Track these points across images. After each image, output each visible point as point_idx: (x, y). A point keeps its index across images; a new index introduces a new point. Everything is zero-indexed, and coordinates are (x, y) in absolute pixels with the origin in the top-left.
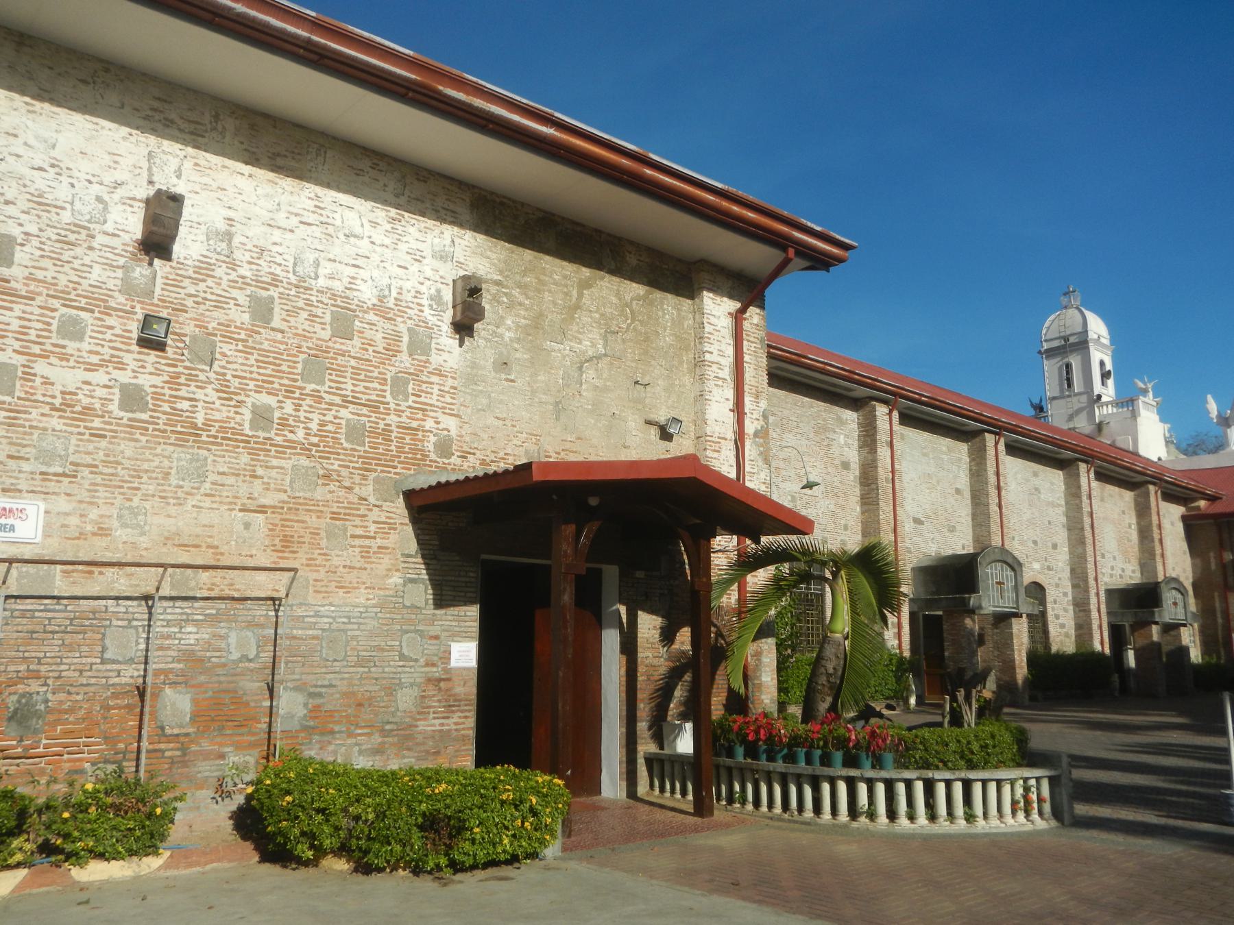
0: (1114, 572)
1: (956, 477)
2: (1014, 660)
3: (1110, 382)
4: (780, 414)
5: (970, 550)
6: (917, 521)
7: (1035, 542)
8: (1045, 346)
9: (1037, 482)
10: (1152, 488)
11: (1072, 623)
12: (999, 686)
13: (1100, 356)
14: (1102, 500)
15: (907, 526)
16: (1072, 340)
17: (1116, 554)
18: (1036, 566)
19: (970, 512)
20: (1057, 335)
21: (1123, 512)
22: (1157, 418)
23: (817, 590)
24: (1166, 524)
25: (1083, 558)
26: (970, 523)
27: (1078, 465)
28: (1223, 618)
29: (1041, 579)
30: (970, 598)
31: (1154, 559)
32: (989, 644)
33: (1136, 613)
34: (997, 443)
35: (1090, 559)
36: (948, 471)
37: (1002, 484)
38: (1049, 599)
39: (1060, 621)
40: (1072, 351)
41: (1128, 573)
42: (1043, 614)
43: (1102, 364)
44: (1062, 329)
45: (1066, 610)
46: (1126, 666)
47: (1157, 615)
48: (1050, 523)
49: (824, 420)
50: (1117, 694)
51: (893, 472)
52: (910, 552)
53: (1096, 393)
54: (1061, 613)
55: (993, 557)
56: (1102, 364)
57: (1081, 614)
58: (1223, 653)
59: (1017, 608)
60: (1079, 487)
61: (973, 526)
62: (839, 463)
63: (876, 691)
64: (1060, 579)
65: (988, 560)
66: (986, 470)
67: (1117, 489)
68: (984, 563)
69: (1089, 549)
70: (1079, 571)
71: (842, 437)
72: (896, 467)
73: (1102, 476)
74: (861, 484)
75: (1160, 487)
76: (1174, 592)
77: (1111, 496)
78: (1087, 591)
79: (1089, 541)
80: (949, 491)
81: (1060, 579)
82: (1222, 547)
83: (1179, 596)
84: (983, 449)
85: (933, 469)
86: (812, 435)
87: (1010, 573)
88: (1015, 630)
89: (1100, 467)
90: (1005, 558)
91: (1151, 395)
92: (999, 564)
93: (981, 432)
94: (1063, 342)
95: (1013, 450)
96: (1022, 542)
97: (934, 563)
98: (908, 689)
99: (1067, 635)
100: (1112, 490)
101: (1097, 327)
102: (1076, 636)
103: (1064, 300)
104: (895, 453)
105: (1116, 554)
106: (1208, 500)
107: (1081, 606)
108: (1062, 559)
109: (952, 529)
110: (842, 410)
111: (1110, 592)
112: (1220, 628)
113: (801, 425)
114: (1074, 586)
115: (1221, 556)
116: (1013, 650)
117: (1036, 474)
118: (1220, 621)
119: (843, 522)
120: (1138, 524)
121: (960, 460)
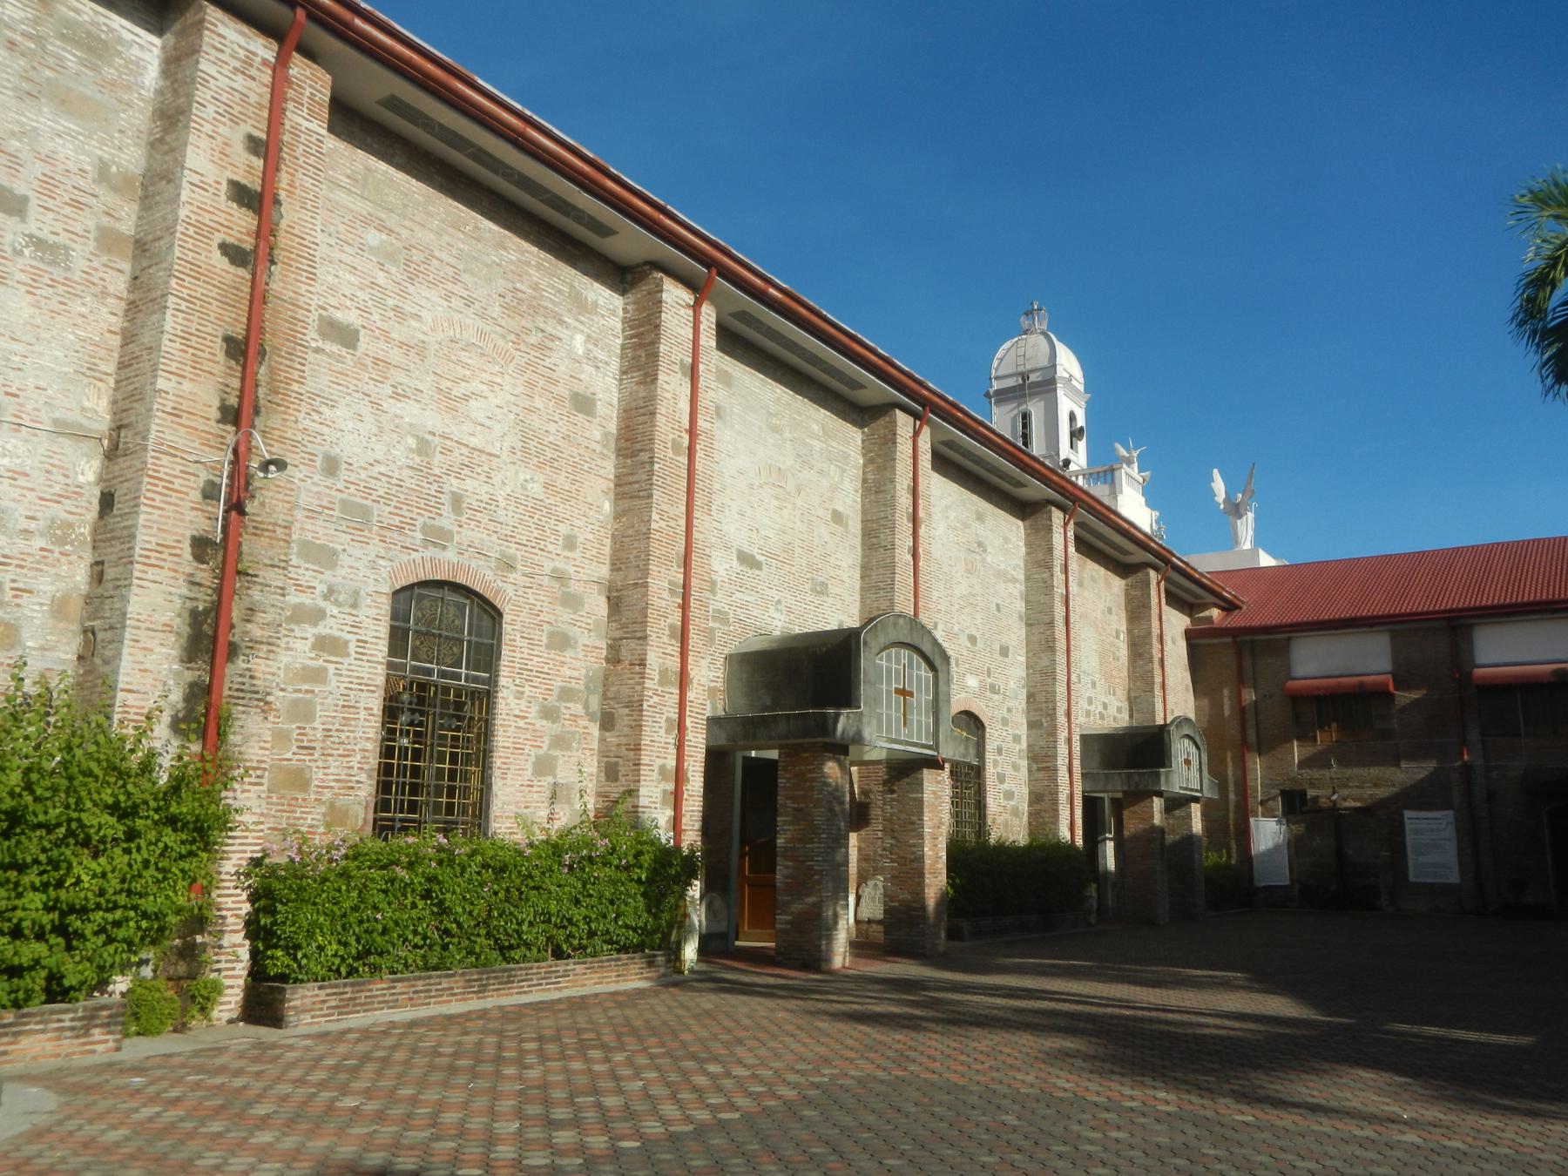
0: (1092, 708)
1: (834, 488)
2: (920, 859)
3: (1082, 445)
4: (405, 233)
5: (853, 622)
6: (746, 560)
7: (972, 639)
8: (996, 385)
9: (982, 531)
10: (1152, 574)
12: (886, 912)
13: (1070, 404)
14: (1081, 584)
15: (721, 565)
16: (1033, 378)
18: (972, 682)
19: (859, 561)
20: (1012, 370)
21: (1110, 611)
22: (1142, 500)
23: (476, 680)
25: (1050, 675)
26: (858, 584)
27: (1050, 511)
28: (1236, 794)
29: (978, 708)
30: (837, 716)
31: (1152, 691)
32: (877, 825)
34: (916, 434)
35: (1062, 677)
36: (821, 472)
37: (921, 514)
38: (990, 746)
39: (1006, 786)
41: (1112, 711)
42: (978, 772)
43: (1072, 417)
44: (1021, 360)
45: (1016, 767)
46: (1101, 868)
47: (1163, 779)
48: (998, 608)
49: (535, 287)
50: (1093, 921)
51: (692, 432)
52: (725, 621)
53: (1063, 457)
54: (1009, 771)
55: (893, 636)
56: (1072, 417)
57: (1041, 775)
58: (1234, 846)
59: (937, 749)
60: (1050, 550)
61: (862, 588)
62: (566, 394)
63: (591, 934)
64: (1009, 710)
65: (883, 639)
66: (892, 481)
67: (1102, 570)
68: (874, 646)
69: (1061, 659)
70: (1041, 697)
71: (579, 338)
72: (702, 423)
73: (1087, 547)
74: (620, 452)
76: (1186, 741)
77: (1094, 580)
78: (1053, 733)
79: (1061, 645)
80: (821, 512)
81: (1009, 710)
82: (1241, 681)
83: (1193, 750)
84: (890, 440)
85: (790, 462)
86: (496, 310)
87: (925, 673)
88: (928, 796)
90: (916, 641)
91: (1136, 466)
92: (904, 653)
93: (887, 408)
94: (1020, 381)
95: (945, 463)
96: (951, 635)
97: (774, 646)
98: (680, 923)
99: (1015, 812)
100: (1095, 570)
101: (1068, 364)
102: (1030, 814)
103: (1025, 322)
104: (701, 395)
105: (1097, 677)
106: (1223, 609)
107: (1041, 760)
108: (1014, 674)
109: (821, 590)
110: (586, 280)
111: (1084, 738)
112: (1232, 808)
113: (466, 278)
114: (1032, 725)
115: (1239, 696)
116: (921, 837)
117: (980, 517)
118: (1232, 796)
119: (564, 529)
120: (1129, 631)
121: (846, 457)
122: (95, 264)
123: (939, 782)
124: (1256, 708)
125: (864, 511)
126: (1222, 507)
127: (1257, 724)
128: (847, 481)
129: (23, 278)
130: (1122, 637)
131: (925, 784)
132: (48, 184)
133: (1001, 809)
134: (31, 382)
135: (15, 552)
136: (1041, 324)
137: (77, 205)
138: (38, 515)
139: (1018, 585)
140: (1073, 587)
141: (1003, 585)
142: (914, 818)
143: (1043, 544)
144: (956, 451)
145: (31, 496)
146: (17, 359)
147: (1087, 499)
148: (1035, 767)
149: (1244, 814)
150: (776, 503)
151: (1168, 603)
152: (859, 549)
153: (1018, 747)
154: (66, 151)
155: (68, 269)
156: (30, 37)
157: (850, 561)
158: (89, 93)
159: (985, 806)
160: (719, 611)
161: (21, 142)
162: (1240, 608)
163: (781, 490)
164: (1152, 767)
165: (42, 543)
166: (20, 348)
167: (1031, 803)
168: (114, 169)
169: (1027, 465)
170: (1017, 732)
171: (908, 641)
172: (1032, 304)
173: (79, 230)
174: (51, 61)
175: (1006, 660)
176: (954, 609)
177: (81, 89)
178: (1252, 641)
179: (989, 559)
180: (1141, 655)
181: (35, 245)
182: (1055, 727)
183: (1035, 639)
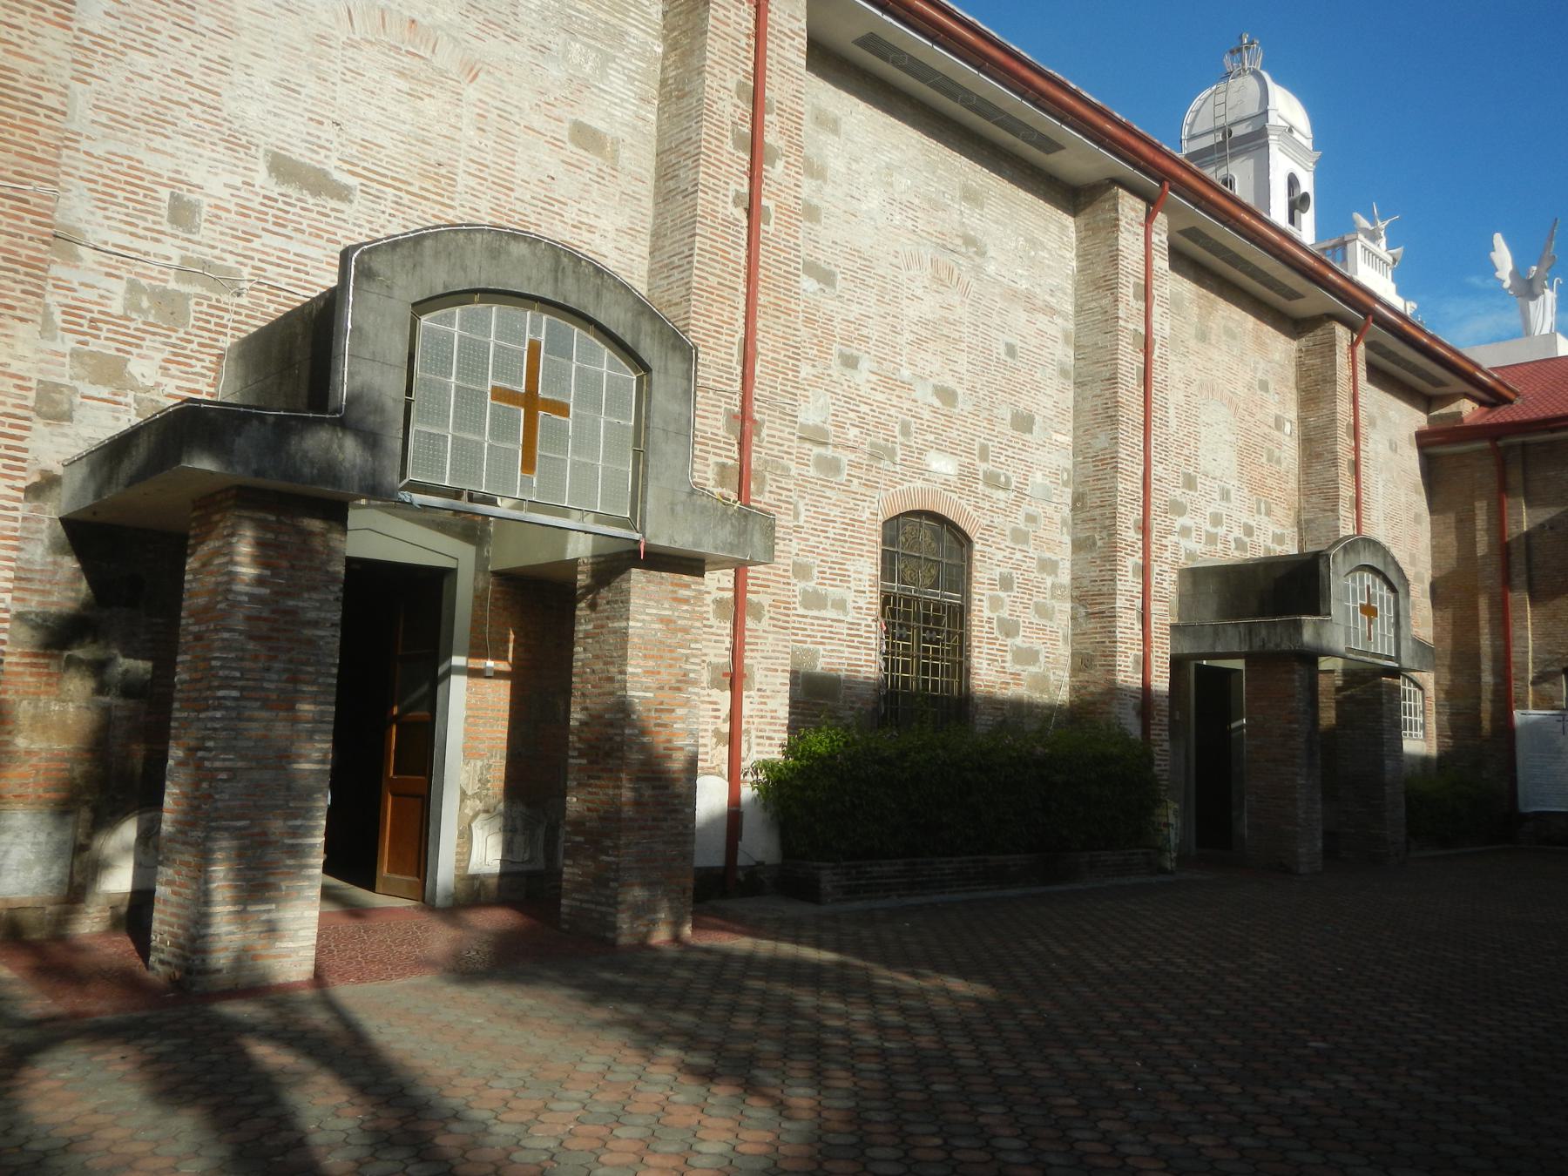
0: (1221, 531)
6: (283, 168)
9: (974, 221)
10: (1342, 333)
11: (1064, 651)
14: (1203, 336)
16: (1238, 131)
17: (1232, 484)
18: (943, 465)
20: (1209, 126)
24: (1375, 446)
27: (1116, 197)
28: (1495, 673)
31: (1335, 510)
33: (1250, 626)
35: (1131, 467)
36: (543, 49)
37: (771, 137)
38: (983, 575)
39: (1019, 641)
40: (1233, 156)
42: (959, 615)
43: (1293, 182)
44: (1220, 110)
45: (1042, 611)
48: (1011, 351)
56: (1293, 182)
57: (1092, 625)
59: (642, 531)
60: (1114, 259)
64: (1031, 518)
65: (439, 279)
69: (1131, 438)
70: (1093, 499)
75: (1370, 346)
76: (1368, 578)
78: (1110, 558)
79: (1132, 410)
80: (537, 121)
83: (1381, 591)
89: (1193, 234)
91: (1383, 242)
92: (535, 326)
101: (1287, 109)
105: (1232, 484)
106: (1482, 403)
114: (1079, 546)
117: (971, 196)
118: (1487, 678)
120: (1302, 420)
123: (686, 601)
124: (1528, 549)
125: (660, 139)
126: (1507, 284)
127: (1529, 570)
128: (616, 82)
130: (1288, 428)
131: (635, 602)
133: (1008, 678)
136: (1254, 59)
139: (1059, 321)
140: (1162, 325)
141: (1024, 316)
142: (613, 670)
143: (1105, 249)
144: (894, 63)
147: (1185, 176)
148: (1082, 611)
149: (1505, 701)
150: (404, 85)
151: (1370, 380)
152: (648, 204)
153: (1049, 581)
157: (623, 222)
159: (968, 671)
160: (205, 264)
162: (1511, 402)
163: (417, 61)
164: (1288, 614)
167: (1075, 671)
169: (1042, 94)
170: (1048, 555)
171: (546, 292)
172: (1241, 38)
175: (1027, 436)
176: (901, 340)
178: (1524, 445)
179: (991, 268)
180: (1319, 455)
182: (1113, 547)
183: (1087, 406)
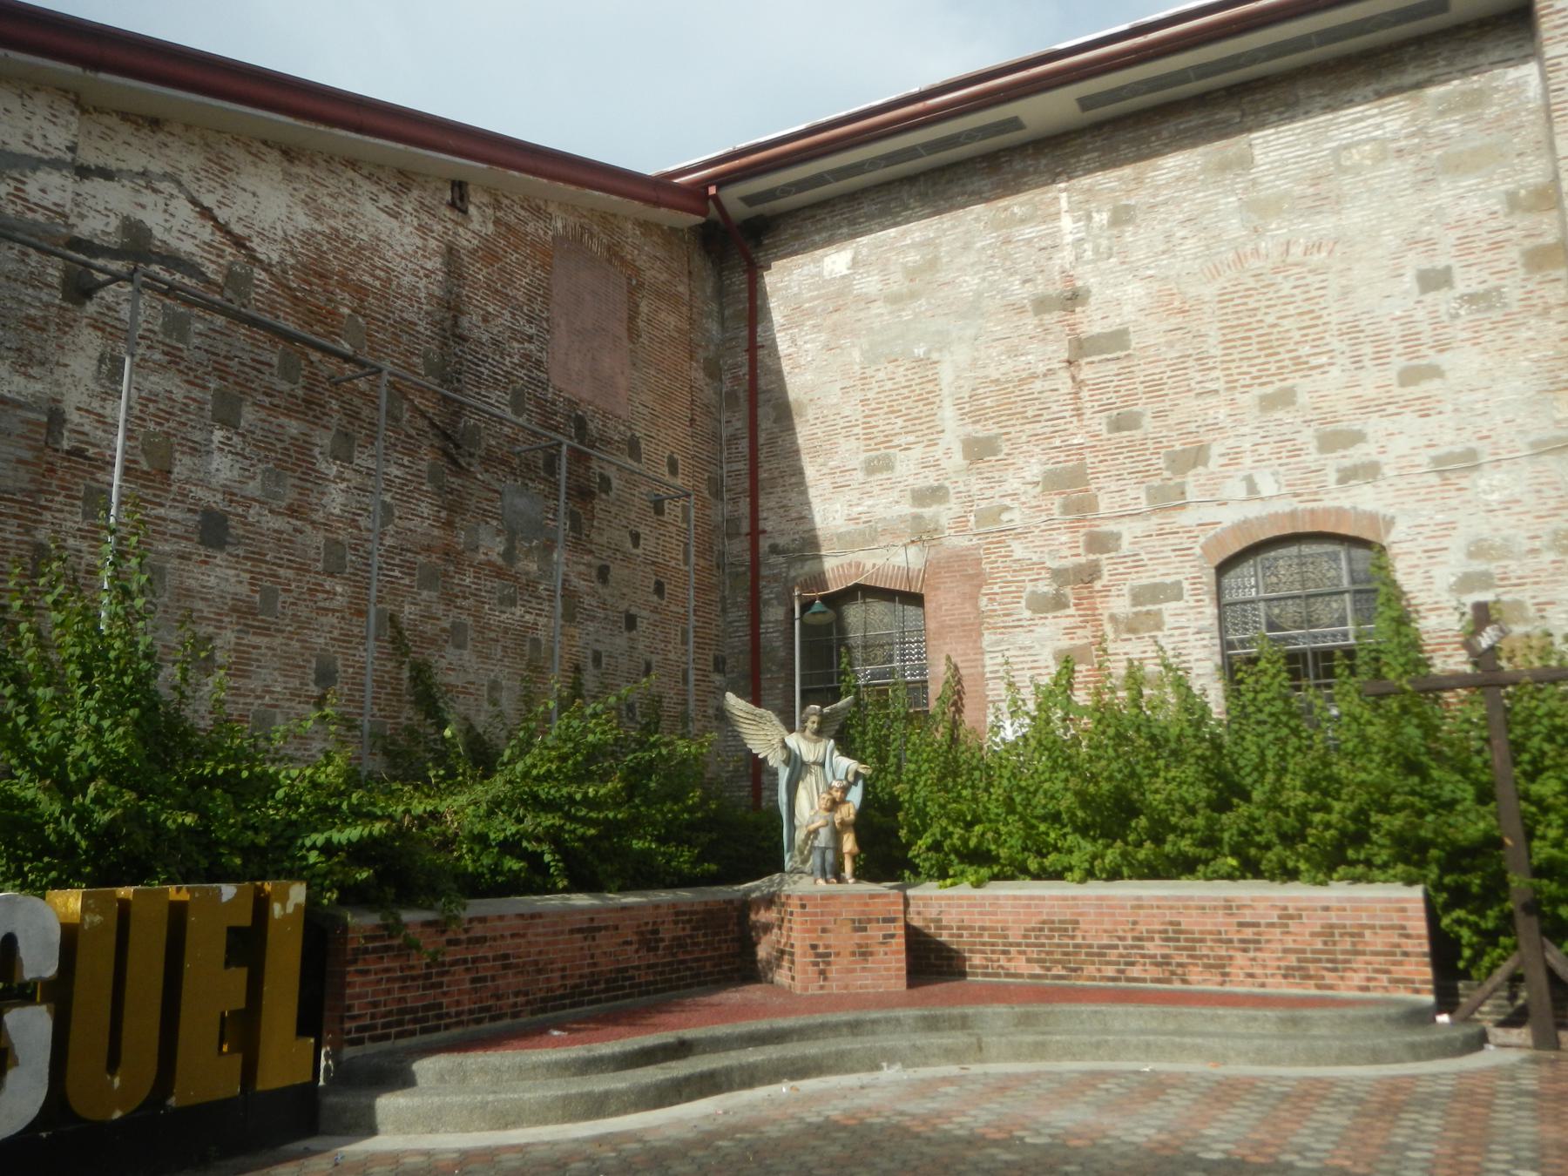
122: (1530, 287)
129: (1465, 335)
132: (1465, 246)
134: (1499, 420)
135: (1527, 572)
137: (1496, 246)
138: (1540, 533)
145: (1528, 518)
146: (1480, 405)
154: (1474, 207)
155: (1505, 305)
156: (1413, 135)
158: (1477, 143)
161: (1429, 224)
165: (1551, 556)
166: (1481, 395)
168: (1523, 192)
173: (1504, 265)
174: (1436, 141)
177: (1472, 144)
181: (1467, 302)
